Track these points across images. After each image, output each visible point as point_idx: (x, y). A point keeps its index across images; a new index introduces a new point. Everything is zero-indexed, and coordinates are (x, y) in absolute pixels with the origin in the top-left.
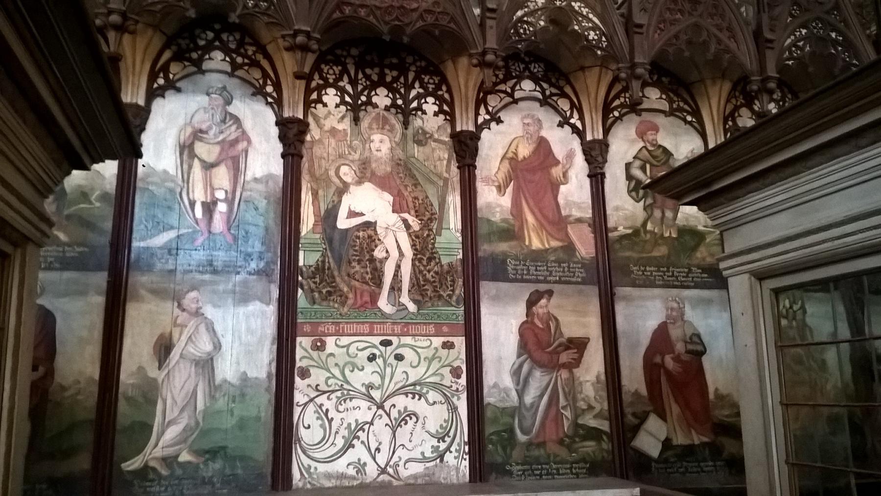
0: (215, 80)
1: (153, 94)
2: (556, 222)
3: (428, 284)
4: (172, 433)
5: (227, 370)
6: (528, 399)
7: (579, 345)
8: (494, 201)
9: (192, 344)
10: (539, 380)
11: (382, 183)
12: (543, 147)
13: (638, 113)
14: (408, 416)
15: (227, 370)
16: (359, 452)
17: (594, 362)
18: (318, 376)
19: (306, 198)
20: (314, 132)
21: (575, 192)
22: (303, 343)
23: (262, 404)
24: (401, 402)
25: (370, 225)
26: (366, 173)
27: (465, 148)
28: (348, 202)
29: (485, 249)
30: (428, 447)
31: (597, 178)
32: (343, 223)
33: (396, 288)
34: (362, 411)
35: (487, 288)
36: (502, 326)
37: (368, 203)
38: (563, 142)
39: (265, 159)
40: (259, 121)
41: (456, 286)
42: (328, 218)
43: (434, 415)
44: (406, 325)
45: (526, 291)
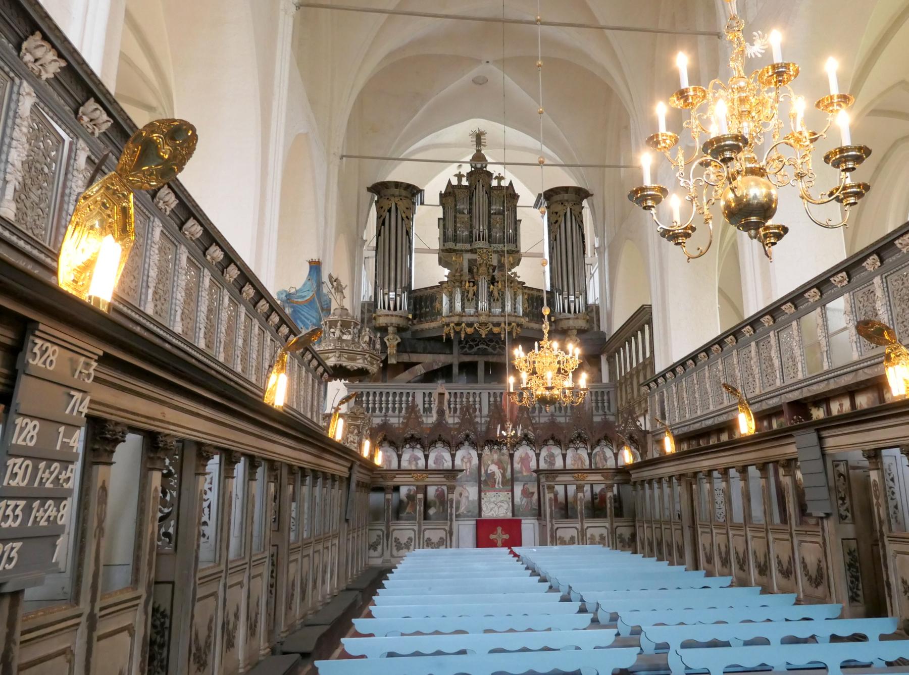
2: (528, 468)
5: (471, 498)
7: (533, 493)
8: (517, 466)
9: (465, 494)
10: (525, 499)
11: (496, 464)
12: (527, 454)
17: (536, 496)
23: (477, 504)
26: (493, 462)
27: (511, 456)
28: (490, 468)
30: (505, 511)
31: (538, 461)
34: (493, 505)
35: (515, 483)
36: (518, 489)
37: (493, 468)
38: (532, 454)
39: (475, 461)
41: (510, 482)
42: (486, 471)
43: (505, 506)
44: (500, 491)
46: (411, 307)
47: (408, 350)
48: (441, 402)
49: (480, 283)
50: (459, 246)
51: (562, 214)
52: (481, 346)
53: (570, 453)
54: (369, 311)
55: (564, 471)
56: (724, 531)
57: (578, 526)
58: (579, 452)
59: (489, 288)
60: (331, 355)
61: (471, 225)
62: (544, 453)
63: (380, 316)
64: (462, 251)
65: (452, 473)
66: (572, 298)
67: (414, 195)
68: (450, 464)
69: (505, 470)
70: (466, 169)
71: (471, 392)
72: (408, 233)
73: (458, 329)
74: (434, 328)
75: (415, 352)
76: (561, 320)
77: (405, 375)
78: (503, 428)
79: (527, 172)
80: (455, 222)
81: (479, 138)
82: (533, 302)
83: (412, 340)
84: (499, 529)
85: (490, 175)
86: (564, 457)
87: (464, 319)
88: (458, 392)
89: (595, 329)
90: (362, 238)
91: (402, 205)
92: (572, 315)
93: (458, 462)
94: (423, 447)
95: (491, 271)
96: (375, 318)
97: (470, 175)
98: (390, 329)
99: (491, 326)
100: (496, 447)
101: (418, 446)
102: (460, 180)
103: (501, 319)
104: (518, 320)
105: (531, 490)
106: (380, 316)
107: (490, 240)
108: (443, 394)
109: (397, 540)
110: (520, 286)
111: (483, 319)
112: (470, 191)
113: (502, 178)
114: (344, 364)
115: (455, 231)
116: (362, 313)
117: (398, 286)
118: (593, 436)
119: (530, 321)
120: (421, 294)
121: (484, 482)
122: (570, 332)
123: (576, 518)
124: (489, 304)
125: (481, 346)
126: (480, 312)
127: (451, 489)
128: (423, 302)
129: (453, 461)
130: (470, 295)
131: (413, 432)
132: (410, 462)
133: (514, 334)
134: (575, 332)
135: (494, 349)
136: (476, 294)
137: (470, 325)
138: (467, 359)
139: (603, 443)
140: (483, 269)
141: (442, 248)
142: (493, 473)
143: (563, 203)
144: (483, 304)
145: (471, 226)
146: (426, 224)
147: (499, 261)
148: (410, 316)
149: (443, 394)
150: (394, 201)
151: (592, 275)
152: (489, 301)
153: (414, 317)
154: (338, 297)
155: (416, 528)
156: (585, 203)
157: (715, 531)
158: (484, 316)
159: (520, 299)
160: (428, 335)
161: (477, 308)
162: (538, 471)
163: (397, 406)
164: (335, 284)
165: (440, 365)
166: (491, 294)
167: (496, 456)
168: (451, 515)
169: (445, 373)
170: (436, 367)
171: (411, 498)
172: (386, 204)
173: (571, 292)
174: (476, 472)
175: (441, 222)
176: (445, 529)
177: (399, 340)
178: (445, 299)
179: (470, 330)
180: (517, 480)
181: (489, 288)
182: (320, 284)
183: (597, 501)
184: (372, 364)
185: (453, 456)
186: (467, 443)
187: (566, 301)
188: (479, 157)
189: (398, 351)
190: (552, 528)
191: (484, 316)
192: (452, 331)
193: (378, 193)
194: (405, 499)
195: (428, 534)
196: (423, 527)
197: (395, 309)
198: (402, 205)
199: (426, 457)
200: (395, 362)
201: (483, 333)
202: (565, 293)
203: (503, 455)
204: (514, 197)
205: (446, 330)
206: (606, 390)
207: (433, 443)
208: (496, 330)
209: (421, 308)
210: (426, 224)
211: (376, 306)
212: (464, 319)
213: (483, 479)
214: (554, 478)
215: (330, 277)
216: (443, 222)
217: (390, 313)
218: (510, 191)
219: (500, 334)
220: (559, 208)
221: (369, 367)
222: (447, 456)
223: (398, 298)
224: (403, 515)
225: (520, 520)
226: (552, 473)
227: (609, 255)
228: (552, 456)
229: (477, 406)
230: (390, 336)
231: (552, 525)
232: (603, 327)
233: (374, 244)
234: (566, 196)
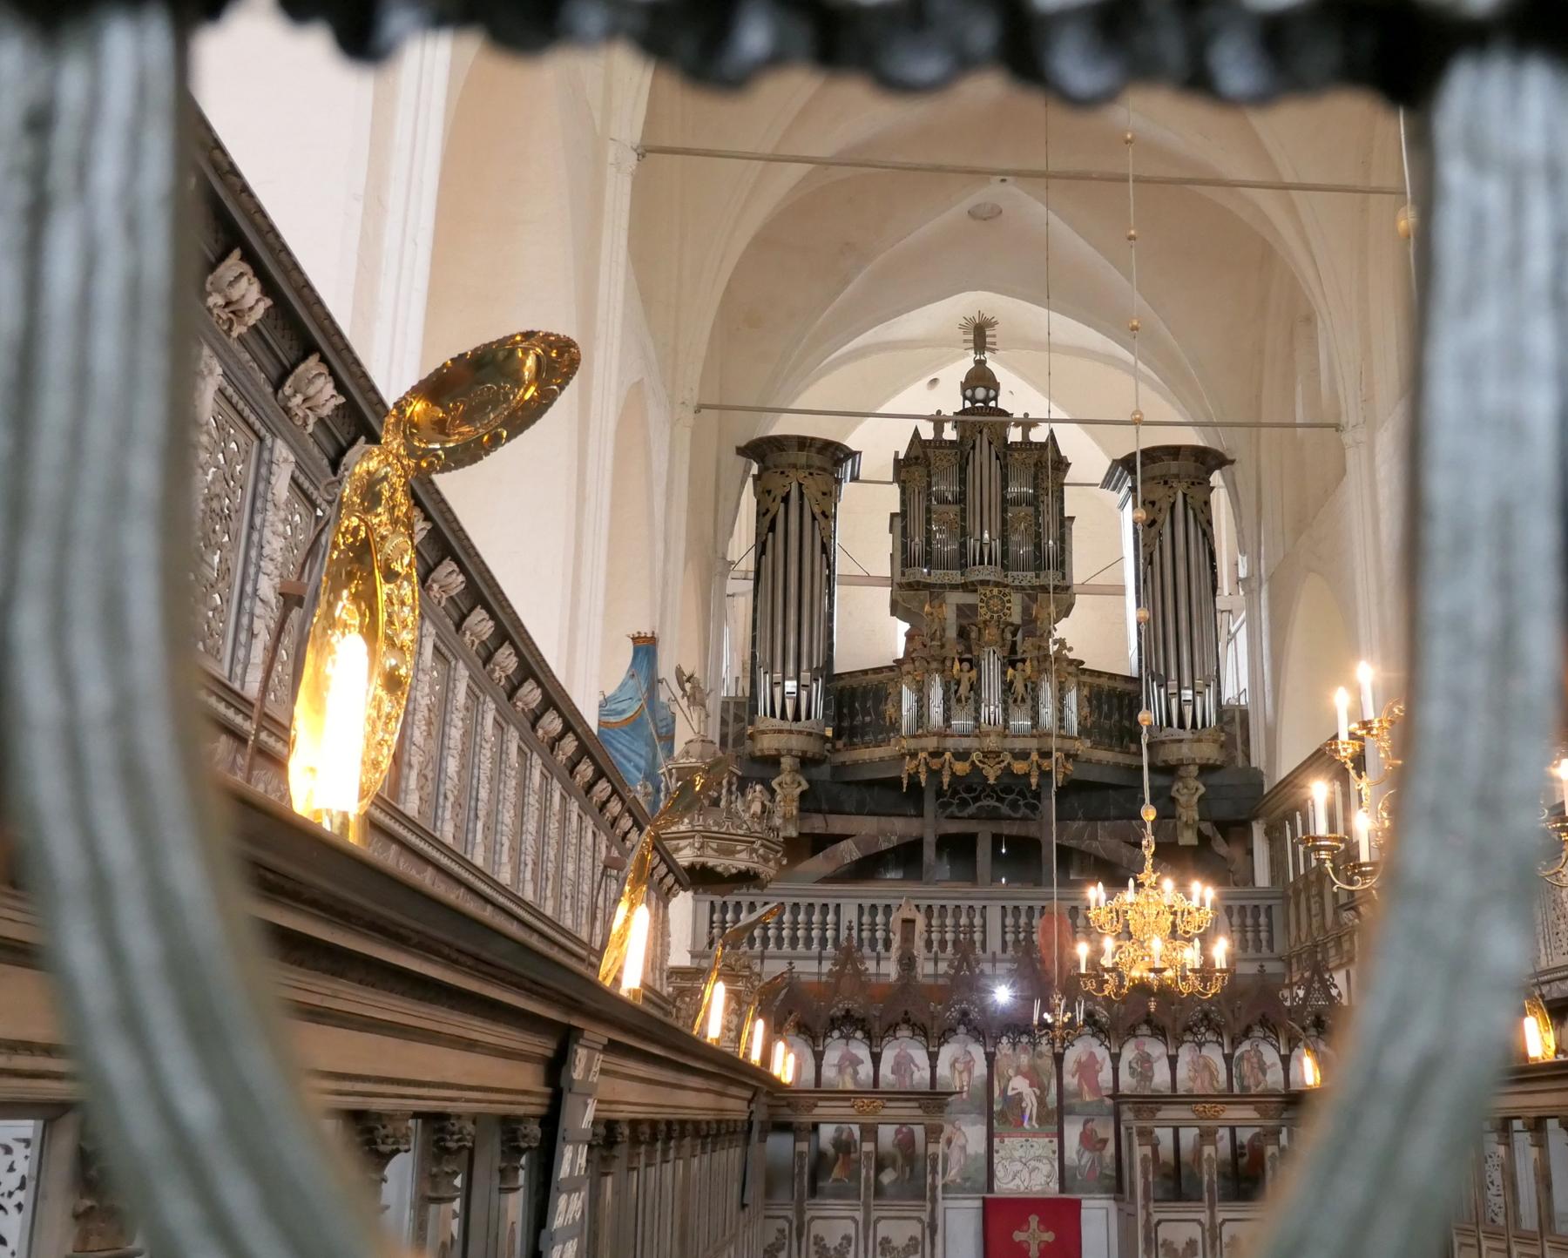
0: (961, 1036)
1: (940, 1045)
2: (1096, 1089)
3: (1041, 1119)
4: (953, 1172)
5: (971, 1150)
6: (1083, 1162)
7: (1104, 1141)
8: (1071, 1081)
10: (1087, 1156)
11: (1025, 1076)
12: (1092, 1055)
13: (1136, 1036)
14: (1035, 1168)
15: (971, 1150)
16: (1017, 1181)
17: (1110, 1148)
18: (1002, 1153)
19: (996, 1083)
20: (998, 1056)
21: (1105, 1076)
22: (996, 1140)
23: (984, 1162)
24: (1033, 1163)
25: (1020, 1094)
26: (1018, 1072)
27: (1059, 1059)
29: (1066, 1102)
30: (1043, 1179)
31: (1116, 1071)
32: (1010, 1093)
33: (1030, 1118)
34: (1018, 1166)
35: (1066, 1118)
36: (1073, 1133)
37: (1019, 1085)
38: (1102, 1053)
39: (980, 1068)
40: (978, 1052)
41: (1055, 1116)
42: (1004, 1091)
43: (1045, 1168)
44: (1035, 1135)
45: (1082, 1119)
46: (831, 713)
47: (825, 807)
48: (907, 938)
50: (938, 576)
51: (1166, 506)
52: (985, 803)
53: (1185, 1055)
54: (738, 719)
55: (1173, 1098)
56: (1504, 1246)
57: (1204, 1217)
58: (1205, 1051)
59: (1004, 673)
60: (683, 843)
61: (963, 528)
62: (1129, 1053)
63: (763, 732)
64: (943, 586)
65: (934, 1099)
66: (1187, 694)
67: (839, 463)
68: (927, 1074)
69: (1044, 1089)
70: (951, 402)
71: (965, 904)
72: (826, 549)
73: (935, 764)
74: (882, 760)
75: (838, 811)
76: (1163, 743)
77: (818, 864)
78: (1047, 1007)
79: (1083, 399)
80: (929, 522)
81: (980, 334)
82: (1099, 707)
83: (831, 788)
84: (1034, 1220)
86: (1173, 1061)
87: (950, 743)
88: (936, 904)
89: (1240, 762)
90: (724, 558)
91: (813, 487)
92: (1187, 734)
93: (943, 1070)
94: (869, 1036)
95: (1009, 636)
96: (751, 737)
97: (960, 420)
98: (786, 762)
99: (1008, 758)
100: (1025, 1039)
101: (859, 1034)
102: (939, 428)
103: (1033, 744)
104: (1068, 744)
105: (1101, 1134)
106: (763, 732)
107: (1006, 561)
108: (913, 921)
109: (819, 1240)
110: (1072, 669)
111: (992, 743)
112: (962, 451)
114: (711, 862)
115: (929, 542)
116: (724, 722)
117: (805, 666)
118: (1235, 1019)
119: (1095, 745)
120: (854, 683)
121: (999, 1115)
122: (1182, 772)
123: (1200, 1200)
124: (1005, 710)
125: (985, 803)
126: (984, 727)
127: (933, 1133)
128: (855, 701)
129: (933, 1068)
130: (963, 690)
131: (848, 1005)
132: (840, 1069)
134: (1194, 770)
135: (1014, 806)
136: (975, 687)
137: (962, 756)
138: (953, 828)
139: (1258, 1032)
140: (991, 633)
141: (898, 578)
142: (1019, 1097)
143: (1169, 481)
144: (992, 710)
145: (964, 533)
146: (865, 524)
147: (1026, 610)
148: (829, 732)
149: (913, 921)
150: (794, 478)
151: (1232, 637)
152: (1005, 702)
153: (838, 734)
154: (695, 716)
155: (859, 1215)
156: (1216, 478)
157: (1485, 1244)
158: (993, 738)
159: (1072, 698)
160: (868, 776)
161: (977, 719)
162: (1116, 1095)
163: (800, 933)
164: (688, 686)
165: (894, 841)
166: (1008, 687)
167: (1024, 1059)
168: (934, 1188)
169: (907, 857)
170: (884, 846)
171: (844, 1146)
172: (778, 484)
173: (1186, 683)
174: (983, 1093)
175: (898, 521)
176: (920, 1220)
177: (805, 786)
178: (908, 699)
179: (961, 768)
180: (1070, 1113)
182: (653, 683)
183: (1244, 1161)
184: (766, 860)
185: (933, 1058)
186: (962, 1029)
187: (1174, 702)
188: (980, 379)
189: (801, 810)
190: (1148, 1221)
191: (993, 738)
192: (922, 769)
193: (761, 459)
194: (831, 1151)
195: (884, 1229)
196: (875, 1215)
197: (797, 718)
198: (813, 487)
199: (876, 1059)
200: (795, 834)
201: (992, 773)
202: (1173, 683)
203: (1041, 1055)
204: (1061, 465)
205: (909, 765)
206: (1263, 904)
207: (891, 1029)
208: (1019, 767)
209: (853, 715)
210: (865, 524)
211: (754, 710)
212: (950, 743)
213: (996, 1108)
214: (1153, 1112)
215: (679, 672)
216: (901, 521)
217: (786, 725)
219: (1027, 775)
220: (1159, 492)
221: (760, 868)
222: (920, 1056)
223: (804, 694)
224: (826, 1184)
225: (1077, 1205)
226: (1148, 1103)
227: (1272, 598)
228: (1146, 1060)
229: (977, 936)
230: (786, 777)
231: (1149, 1215)
232: (1258, 759)
233: (748, 564)
234: (1174, 466)
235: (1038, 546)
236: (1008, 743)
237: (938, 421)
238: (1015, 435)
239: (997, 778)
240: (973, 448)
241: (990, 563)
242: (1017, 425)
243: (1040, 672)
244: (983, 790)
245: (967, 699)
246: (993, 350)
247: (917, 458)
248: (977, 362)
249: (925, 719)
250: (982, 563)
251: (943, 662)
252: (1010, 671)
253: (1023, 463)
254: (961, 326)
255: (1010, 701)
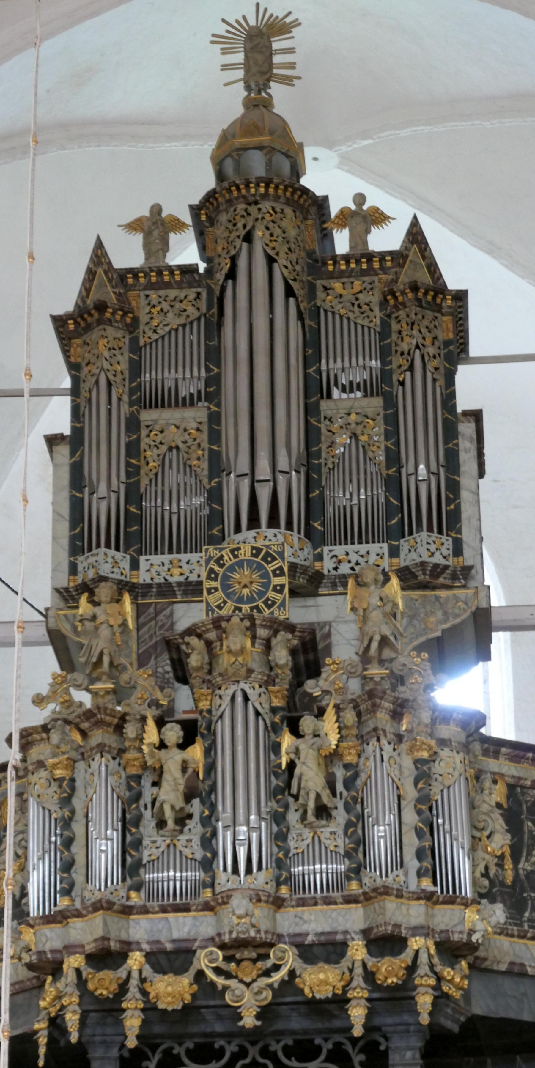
49: (223, 730)
64: (166, 590)
73: (104, 983)
85: (314, 207)
87: (141, 929)
97: (206, 214)
99: (291, 959)
103: (351, 919)
104: (446, 918)
107: (316, 524)
111: (243, 915)
112: (212, 290)
113: (378, 218)
115: (134, 494)
126: (224, 880)
133: (424, 1001)
136: (201, 789)
137: (172, 959)
144: (243, 834)
145: (217, 467)
152: (278, 818)
161: (207, 864)
175: (64, 450)
179: (172, 990)
181: (276, 748)
192: (72, 1000)
201: (248, 1000)
208: (320, 980)
212: (141, 929)
218: (415, 272)
219: (341, 1001)
235: (393, 484)
236: (289, 921)
237: (155, 228)
238: (342, 242)
239: (264, 1013)
240: (232, 275)
241: (273, 522)
242: (342, 226)
243: (362, 739)
244: (242, 1053)
245: (182, 820)
246: (288, 81)
247: (101, 307)
248: (250, 104)
249: (78, 875)
250: (254, 522)
251: (119, 729)
252: (287, 741)
253: (355, 303)
254: (217, 39)
255: (293, 817)
